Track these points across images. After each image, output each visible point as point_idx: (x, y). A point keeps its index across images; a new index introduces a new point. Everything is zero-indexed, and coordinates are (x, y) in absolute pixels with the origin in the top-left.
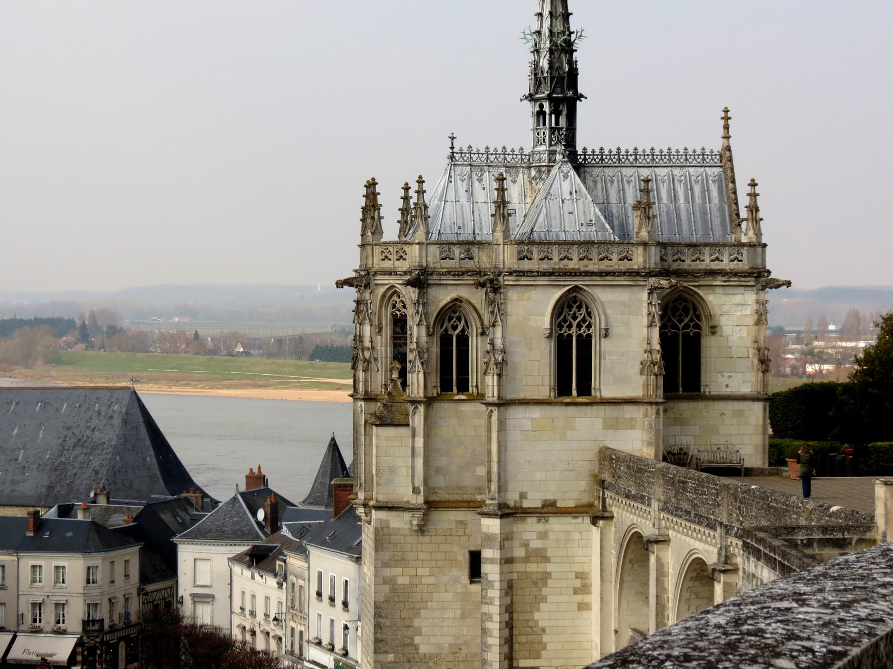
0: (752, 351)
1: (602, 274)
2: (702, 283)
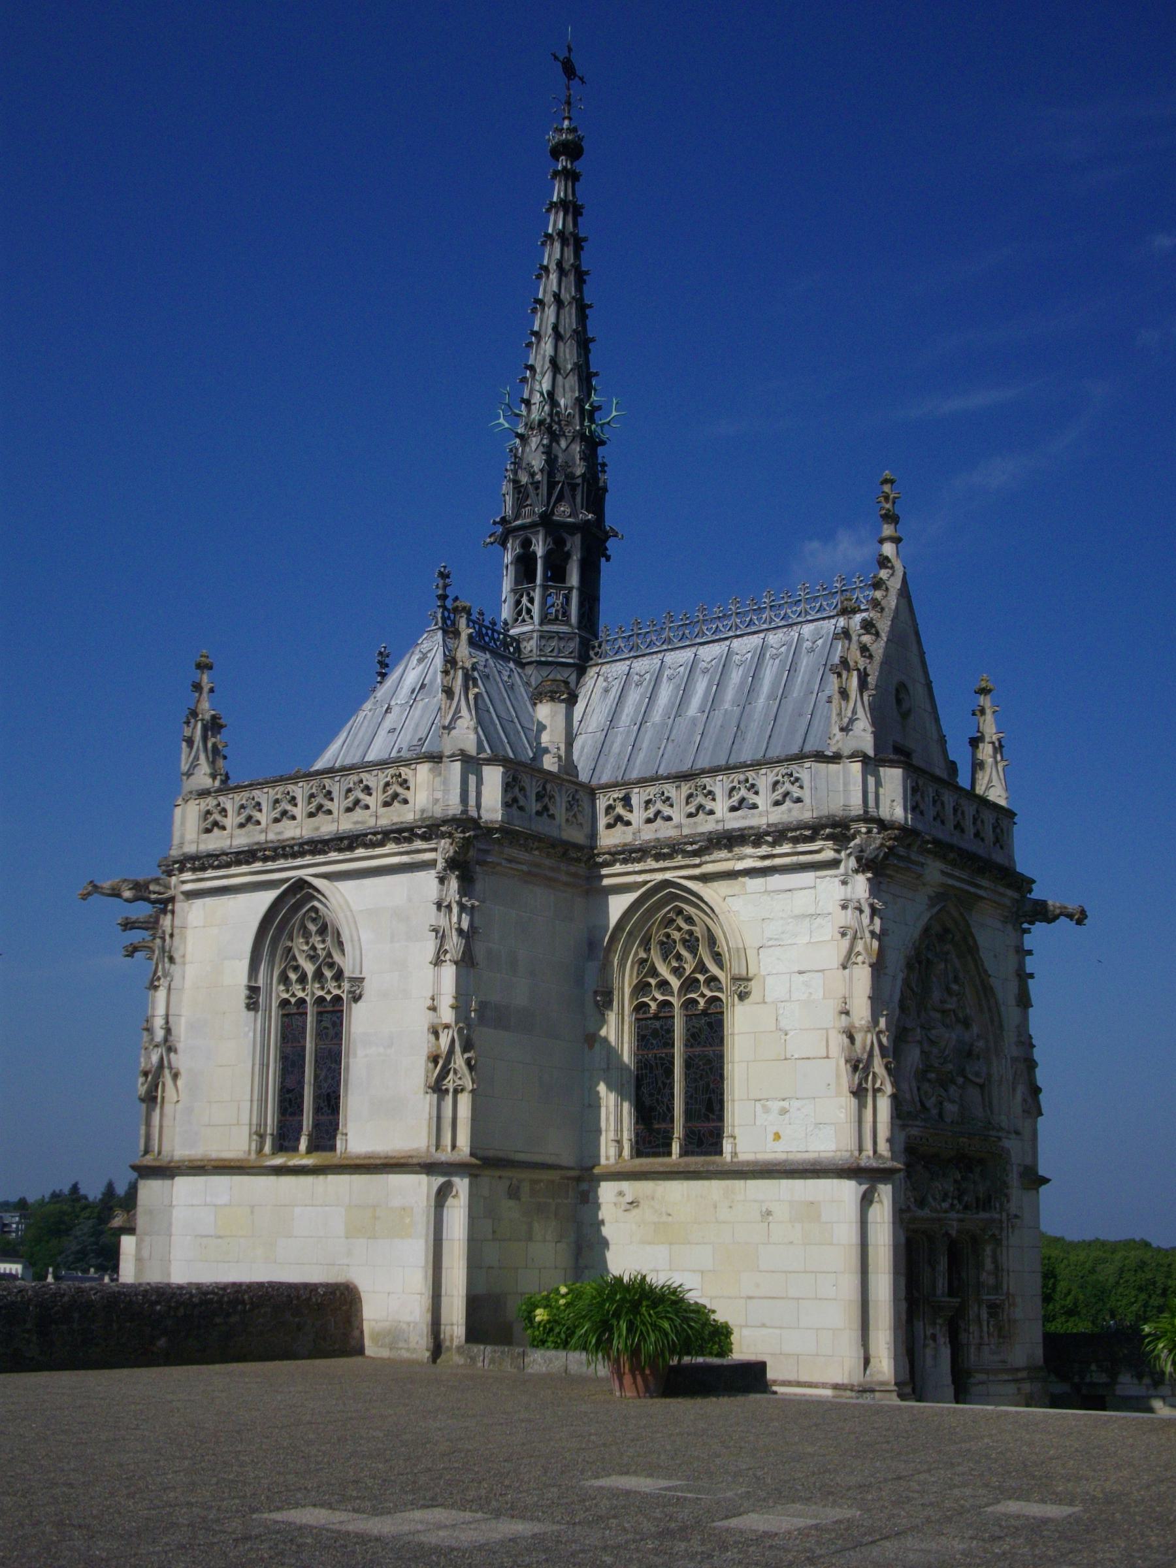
0: (838, 1041)
1: (348, 842)
2: (709, 868)
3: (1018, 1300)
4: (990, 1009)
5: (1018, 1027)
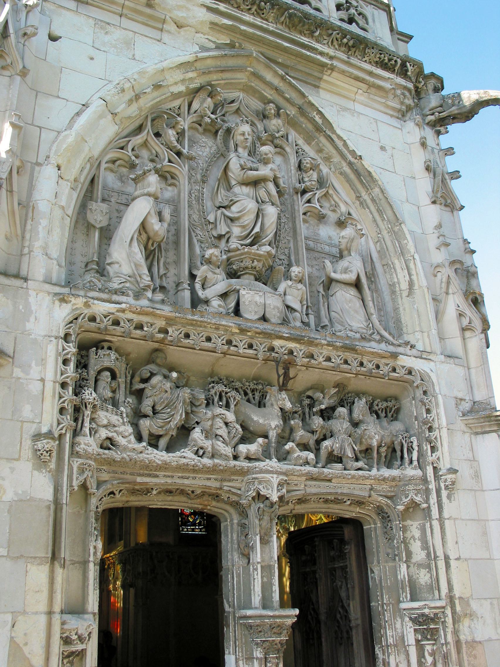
3: (474, 605)
4: (373, 200)
5: (439, 226)
